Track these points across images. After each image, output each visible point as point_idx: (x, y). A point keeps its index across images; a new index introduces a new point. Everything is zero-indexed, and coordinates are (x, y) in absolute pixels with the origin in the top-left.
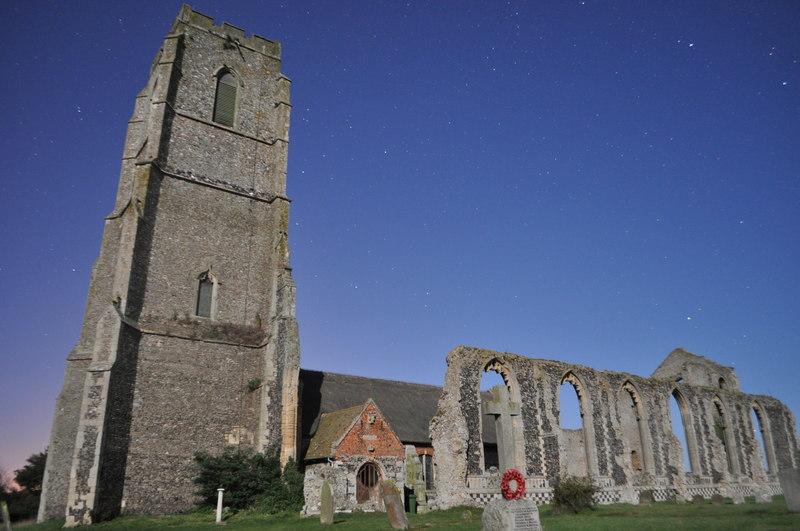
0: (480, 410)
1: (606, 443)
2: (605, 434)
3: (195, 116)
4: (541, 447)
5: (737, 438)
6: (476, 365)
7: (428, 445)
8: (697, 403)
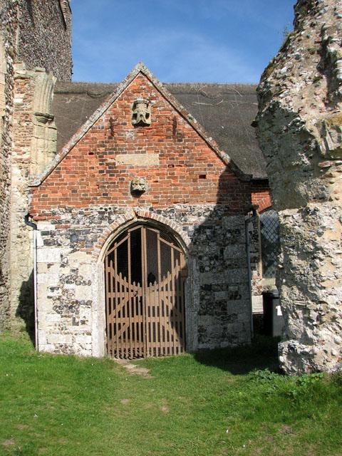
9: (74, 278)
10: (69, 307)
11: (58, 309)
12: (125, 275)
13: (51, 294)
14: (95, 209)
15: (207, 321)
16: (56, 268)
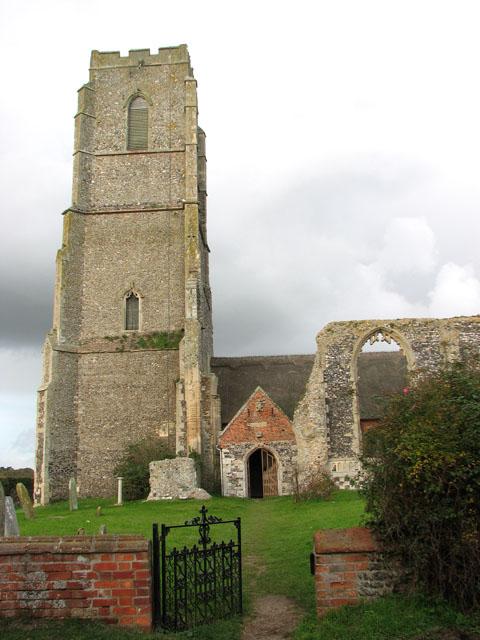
3: (111, 151)
9: (236, 469)
11: (230, 481)
15: (286, 485)
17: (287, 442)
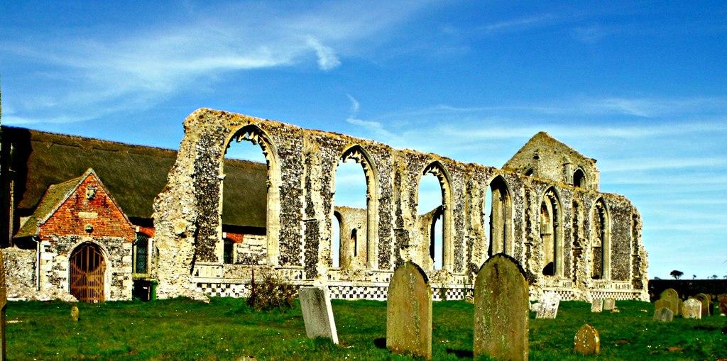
0: (221, 187)
1: (392, 233)
2: (393, 222)
4: (302, 233)
5: (567, 238)
6: (220, 132)
7: (149, 223)
8: (523, 195)
9: (58, 267)
10: (55, 281)
11: (51, 281)
12: (79, 267)
13: (47, 274)
14: (69, 236)
15: (115, 289)
16: (50, 262)
17: (120, 238)
